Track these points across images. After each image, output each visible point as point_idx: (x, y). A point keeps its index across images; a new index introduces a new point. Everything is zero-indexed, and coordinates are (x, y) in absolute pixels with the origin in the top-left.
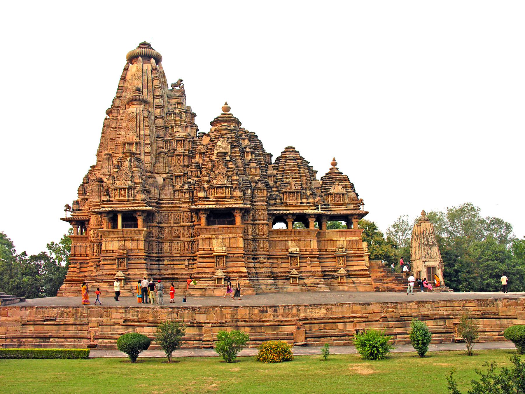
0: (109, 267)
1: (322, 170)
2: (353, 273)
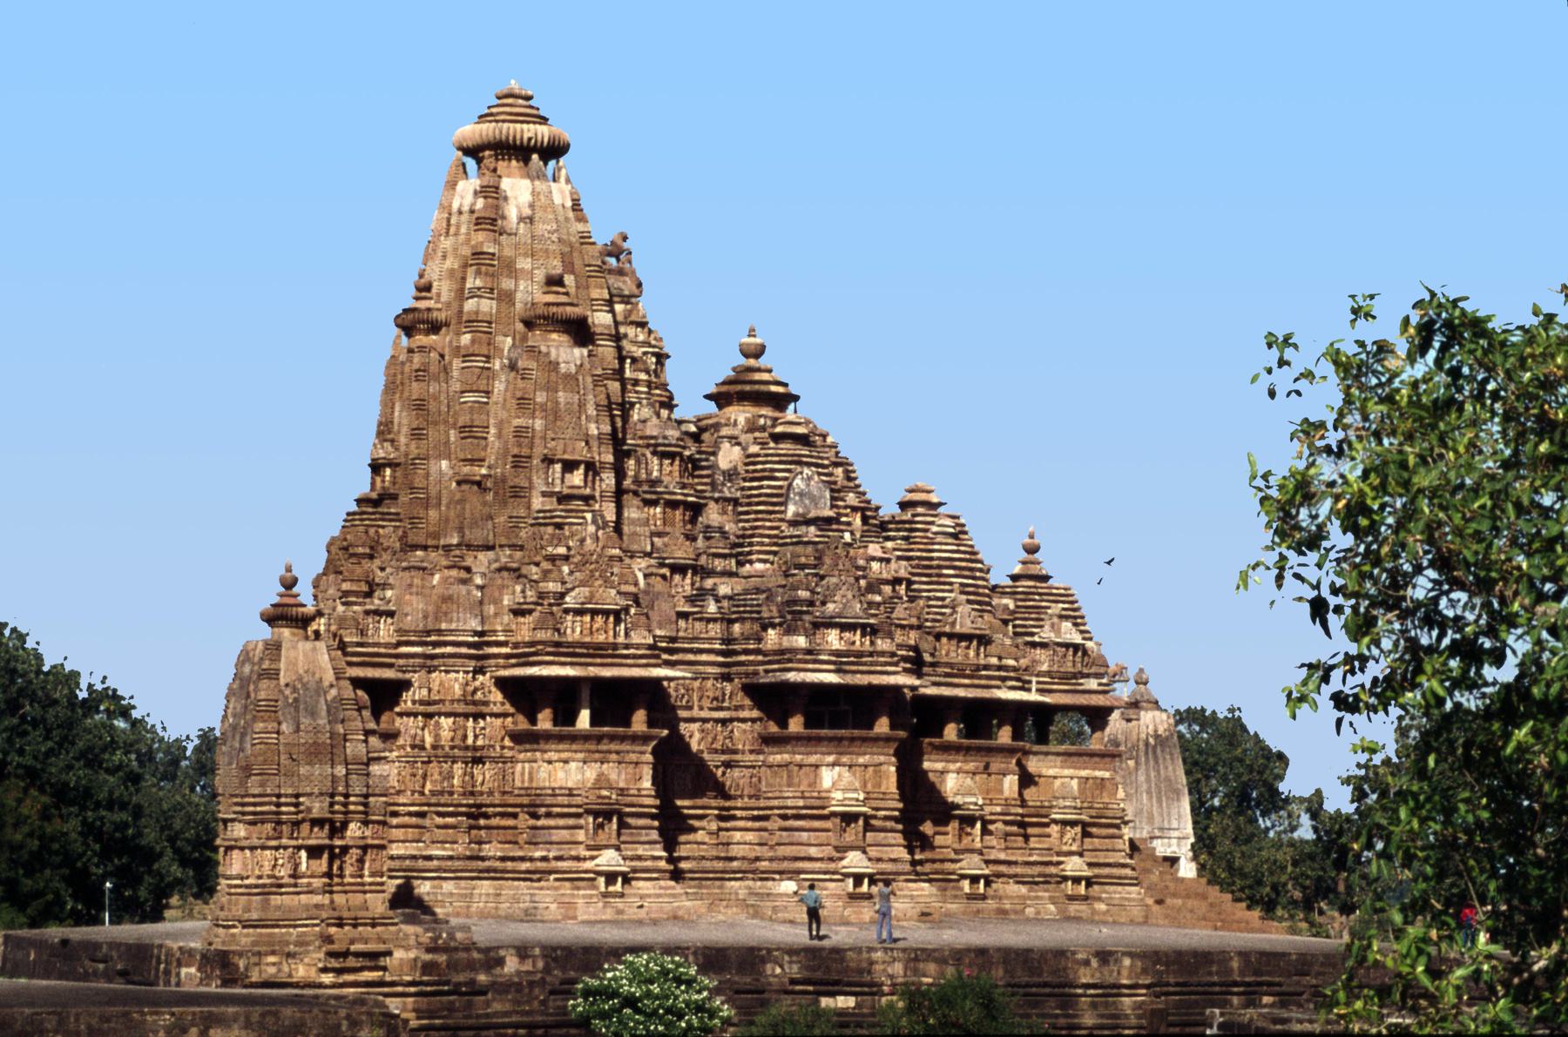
0: (564, 835)
1: (1002, 564)
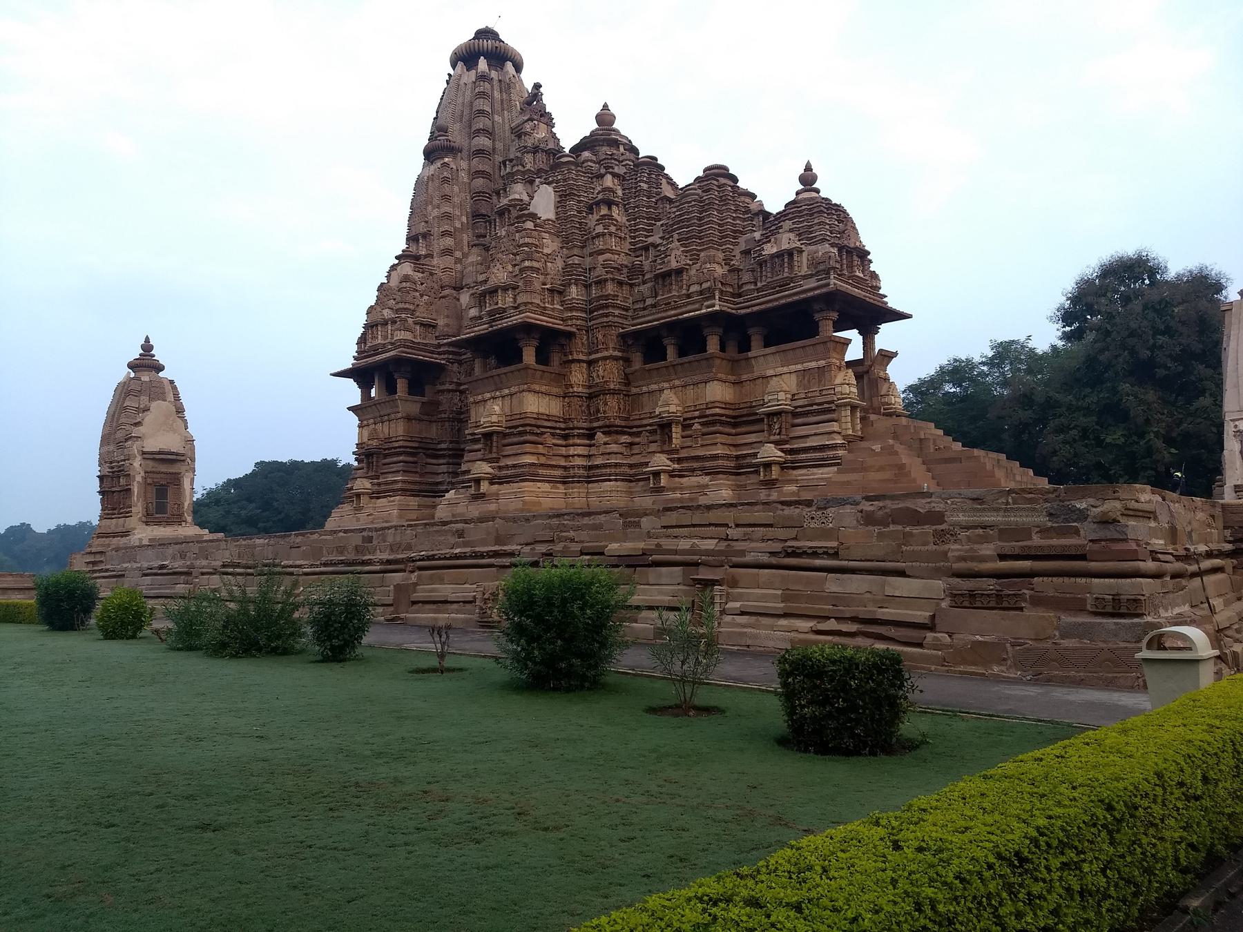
2: (803, 456)
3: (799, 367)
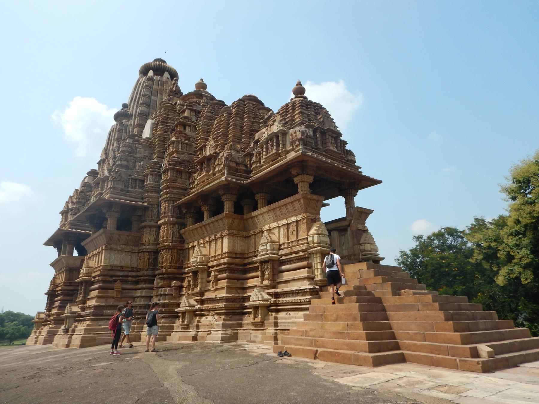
3: (284, 222)
